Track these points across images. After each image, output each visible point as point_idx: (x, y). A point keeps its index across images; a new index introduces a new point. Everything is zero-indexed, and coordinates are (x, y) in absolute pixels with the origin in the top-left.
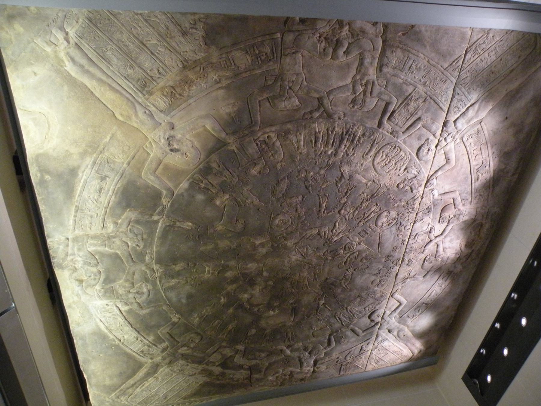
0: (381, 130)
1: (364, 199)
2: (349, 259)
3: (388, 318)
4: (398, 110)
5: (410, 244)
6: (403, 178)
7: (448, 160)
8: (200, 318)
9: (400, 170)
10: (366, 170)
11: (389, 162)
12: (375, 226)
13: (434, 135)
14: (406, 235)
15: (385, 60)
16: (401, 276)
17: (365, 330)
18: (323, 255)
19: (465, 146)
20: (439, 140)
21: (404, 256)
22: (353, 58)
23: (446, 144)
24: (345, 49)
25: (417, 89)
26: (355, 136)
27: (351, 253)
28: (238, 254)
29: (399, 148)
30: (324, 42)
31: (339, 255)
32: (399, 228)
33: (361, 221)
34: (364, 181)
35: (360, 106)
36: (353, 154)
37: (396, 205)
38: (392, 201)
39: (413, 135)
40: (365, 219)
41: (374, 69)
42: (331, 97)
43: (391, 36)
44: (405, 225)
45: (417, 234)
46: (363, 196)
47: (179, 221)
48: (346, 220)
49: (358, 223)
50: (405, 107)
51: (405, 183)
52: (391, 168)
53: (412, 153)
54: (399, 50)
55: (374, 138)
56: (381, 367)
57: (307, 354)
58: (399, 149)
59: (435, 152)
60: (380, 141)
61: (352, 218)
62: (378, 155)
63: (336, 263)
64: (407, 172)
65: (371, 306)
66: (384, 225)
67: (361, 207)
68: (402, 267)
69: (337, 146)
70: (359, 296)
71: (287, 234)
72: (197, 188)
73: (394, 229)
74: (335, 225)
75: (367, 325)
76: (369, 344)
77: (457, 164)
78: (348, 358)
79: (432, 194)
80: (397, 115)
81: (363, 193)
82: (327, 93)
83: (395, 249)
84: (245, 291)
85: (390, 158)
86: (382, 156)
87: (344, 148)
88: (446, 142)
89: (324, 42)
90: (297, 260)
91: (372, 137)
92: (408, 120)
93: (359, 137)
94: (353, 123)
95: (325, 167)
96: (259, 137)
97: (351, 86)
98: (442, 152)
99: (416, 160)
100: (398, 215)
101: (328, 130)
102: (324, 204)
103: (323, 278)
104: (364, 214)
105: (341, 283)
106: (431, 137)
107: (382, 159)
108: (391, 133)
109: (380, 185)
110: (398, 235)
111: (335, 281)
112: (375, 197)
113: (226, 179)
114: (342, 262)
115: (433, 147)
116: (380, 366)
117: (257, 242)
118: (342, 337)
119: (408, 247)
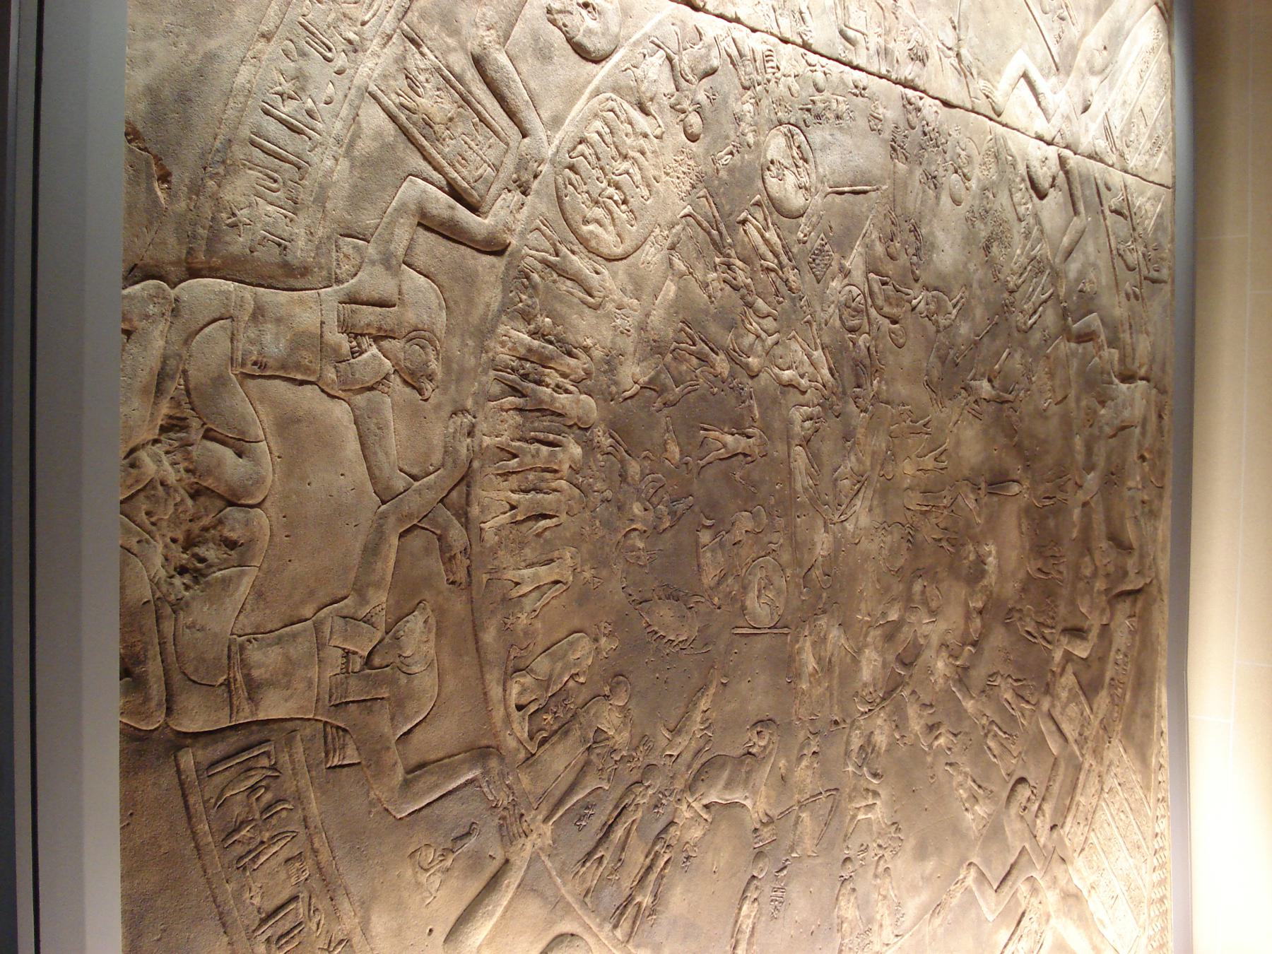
0: (514, 241)
2: (886, 309)
3: (1053, 121)
4: (449, 169)
8: (975, 799)
9: (646, 136)
10: (637, 285)
11: (618, 187)
12: (803, 220)
15: (267, 254)
16: (952, 88)
17: (1074, 204)
18: (865, 411)
22: (259, 407)
24: (229, 454)
25: (373, 88)
27: (869, 300)
28: (836, 723)
30: (201, 551)
31: (873, 350)
32: (818, 117)
33: (786, 282)
34: (670, 289)
35: (430, 349)
36: (586, 349)
37: (750, 138)
38: (737, 156)
40: (780, 263)
41: (302, 302)
42: (400, 482)
43: (172, 241)
44: (812, 90)
46: (716, 284)
49: (790, 289)
50: (437, 139)
51: (686, 104)
52: (638, 178)
53: (591, 87)
54: (228, 195)
56: (1170, 127)
57: (1103, 412)
64: (652, 100)
65: (1018, 196)
66: (805, 180)
67: (747, 286)
68: (927, 87)
70: (987, 248)
74: (790, 385)
75: (1062, 200)
76: (1110, 184)
78: (1132, 258)
80: (465, 172)
82: (384, 503)
84: (930, 671)
85: (605, 183)
87: (567, 391)
89: (201, 551)
91: (535, 276)
92: (482, 120)
93: (532, 334)
94: (485, 372)
97: (360, 400)
101: (506, 475)
107: (607, 221)
109: (685, 216)
111: (938, 349)
112: (720, 234)
116: (1167, 134)
118: (1081, 291)
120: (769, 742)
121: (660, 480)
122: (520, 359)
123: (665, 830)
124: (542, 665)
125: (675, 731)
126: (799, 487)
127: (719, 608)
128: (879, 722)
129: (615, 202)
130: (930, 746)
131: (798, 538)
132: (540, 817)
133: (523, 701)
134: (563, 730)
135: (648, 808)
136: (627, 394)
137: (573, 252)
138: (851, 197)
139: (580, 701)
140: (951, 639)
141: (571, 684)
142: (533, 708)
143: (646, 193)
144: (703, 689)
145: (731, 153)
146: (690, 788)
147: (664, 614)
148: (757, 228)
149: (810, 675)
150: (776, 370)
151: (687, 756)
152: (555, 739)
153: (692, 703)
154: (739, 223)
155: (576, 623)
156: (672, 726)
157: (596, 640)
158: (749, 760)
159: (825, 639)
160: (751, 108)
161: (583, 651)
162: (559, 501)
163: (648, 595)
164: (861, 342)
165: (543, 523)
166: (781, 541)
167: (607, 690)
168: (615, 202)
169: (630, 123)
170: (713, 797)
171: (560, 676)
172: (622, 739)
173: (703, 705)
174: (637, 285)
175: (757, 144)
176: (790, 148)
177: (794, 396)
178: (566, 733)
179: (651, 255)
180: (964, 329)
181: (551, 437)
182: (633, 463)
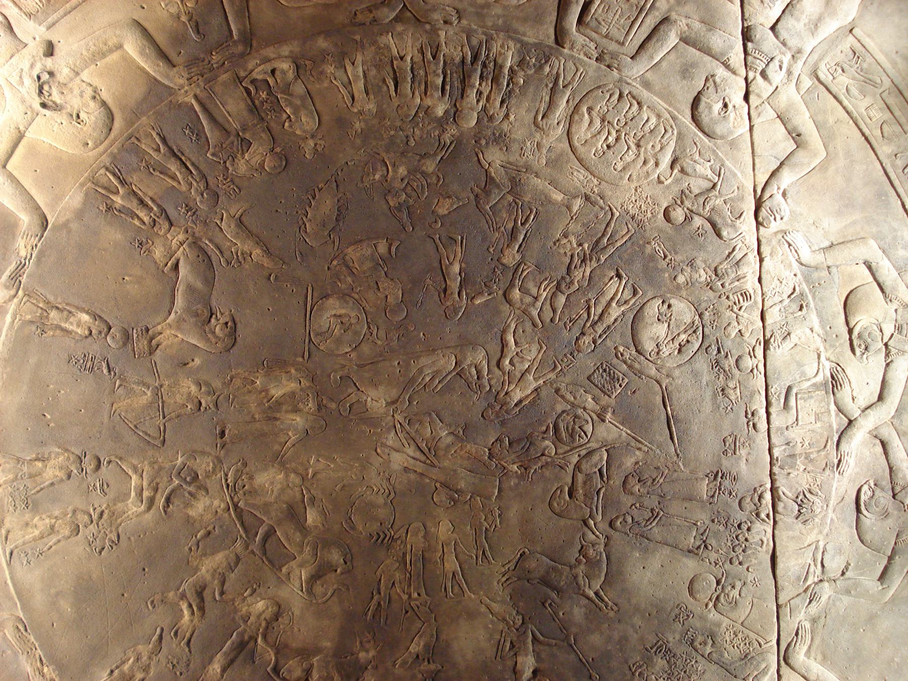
1: (572, 256)
2: (580, 478)
5: (779, 429)
6: (676, 189)
7: (797, 137)
10: (555, 162)
13: (727, 66)
14: (752, 395)
16: (789, 565)
18: (491, 456)
19: (835, 97)
20: (746, 79)
21: (771, 474)
23: (772, 89)
26: (498, 67)
27: (583, 453)
28: (223, 434)
29: (634, 98)
33: (583, 334)
34: (558, 197)
36: (507, 116)
37: (681, 279)
39: (664, 64)
45: (789, 389)
47: (57, 308)
48: (534, 325)
49: (577, 339)
51: (688, 204)
55: (555, 72)
58: (635, 103)
59: (749, 114)
60: (573, 79)
61: (552, 320)
62: (576, 117)
63: (538, 490)
64: (682, 171)
66: (665, 351)
67: (572, 282)
68: (780, 525)
69: (457, 93)
71: (360, 366)
72: (103, 208)
73: (702, 365)
74: (504, 345)
77: (831, 148)
79: (790, 245)
81: (566, 236)
83: (730, 446)
84: (254, 585)
85: (617, 128)
86: (591, 122)
87: (478, 101)
88: (771, 84)
90: (406, 469)
91: (547, 69)
93: (511, 68)
95: (435, 154)
96: (252, 71)
98: (769, 113)
99: (695, 134)
100: (700, 316)
102: (456, 268)
103: (510, 554)
104: (589, 308)
105: (575, 577)
106: (721, 72)
108: (597, 59)
110: (723, 390)
113: (175, 184)
114: (561, 489)
115: (737, 98)
117: (277, 392)
119: (774, 440)
120: (217, 337)
121: (423, 193)
122: (495, 60)
123: (168, 218)
124: (299, 89)
125: (240, 222)
126: (424, 361)
127: (329, 268)
128: (216, 503)
129: (607, 138)
130: (183, 596)
131: (381, 364)
132: (198, 92)
133: (277, 73)
134: (254, 109)
135: (187, 198)
136: (481, 156)
137: (568, 102)
138: (663, 417)
139: (273, 124)
140: (283, 620)
141: (285, 116)
142: (271, 81)
143: (619, 166)
144: (268, 252)
145: (665, 257)
146: (195, 243)
147: (327, 205)
148: (617, 291)
149: (267, 391)
150: (513, 326)
151: (219, 239)
152: (249, 102)
153: (260, 241)
154: (617, 270)
155: (325, 118)
156: (244, 219)
157: (313, 137)
158: (207, 314)
159: (296, 410)
160: (703, 279)
161: (307, 122)
162: (406, 96)
163: (341, 189)
164: (547, 442)
165: (392, 88)
166: (379, 342)
167: (278, 150)
168: (607, 138)
169: (661, 149)
170: (183, 270)
171: (290, 104)
172: (242, 167)
173: (257, 252)
174: (555, 162)
175: (678, 288)
177: (495, 348)
178: (251, 111)
179: (579, 177)
180: (578, 613)
181: (448, 88)
182: (434, 166)
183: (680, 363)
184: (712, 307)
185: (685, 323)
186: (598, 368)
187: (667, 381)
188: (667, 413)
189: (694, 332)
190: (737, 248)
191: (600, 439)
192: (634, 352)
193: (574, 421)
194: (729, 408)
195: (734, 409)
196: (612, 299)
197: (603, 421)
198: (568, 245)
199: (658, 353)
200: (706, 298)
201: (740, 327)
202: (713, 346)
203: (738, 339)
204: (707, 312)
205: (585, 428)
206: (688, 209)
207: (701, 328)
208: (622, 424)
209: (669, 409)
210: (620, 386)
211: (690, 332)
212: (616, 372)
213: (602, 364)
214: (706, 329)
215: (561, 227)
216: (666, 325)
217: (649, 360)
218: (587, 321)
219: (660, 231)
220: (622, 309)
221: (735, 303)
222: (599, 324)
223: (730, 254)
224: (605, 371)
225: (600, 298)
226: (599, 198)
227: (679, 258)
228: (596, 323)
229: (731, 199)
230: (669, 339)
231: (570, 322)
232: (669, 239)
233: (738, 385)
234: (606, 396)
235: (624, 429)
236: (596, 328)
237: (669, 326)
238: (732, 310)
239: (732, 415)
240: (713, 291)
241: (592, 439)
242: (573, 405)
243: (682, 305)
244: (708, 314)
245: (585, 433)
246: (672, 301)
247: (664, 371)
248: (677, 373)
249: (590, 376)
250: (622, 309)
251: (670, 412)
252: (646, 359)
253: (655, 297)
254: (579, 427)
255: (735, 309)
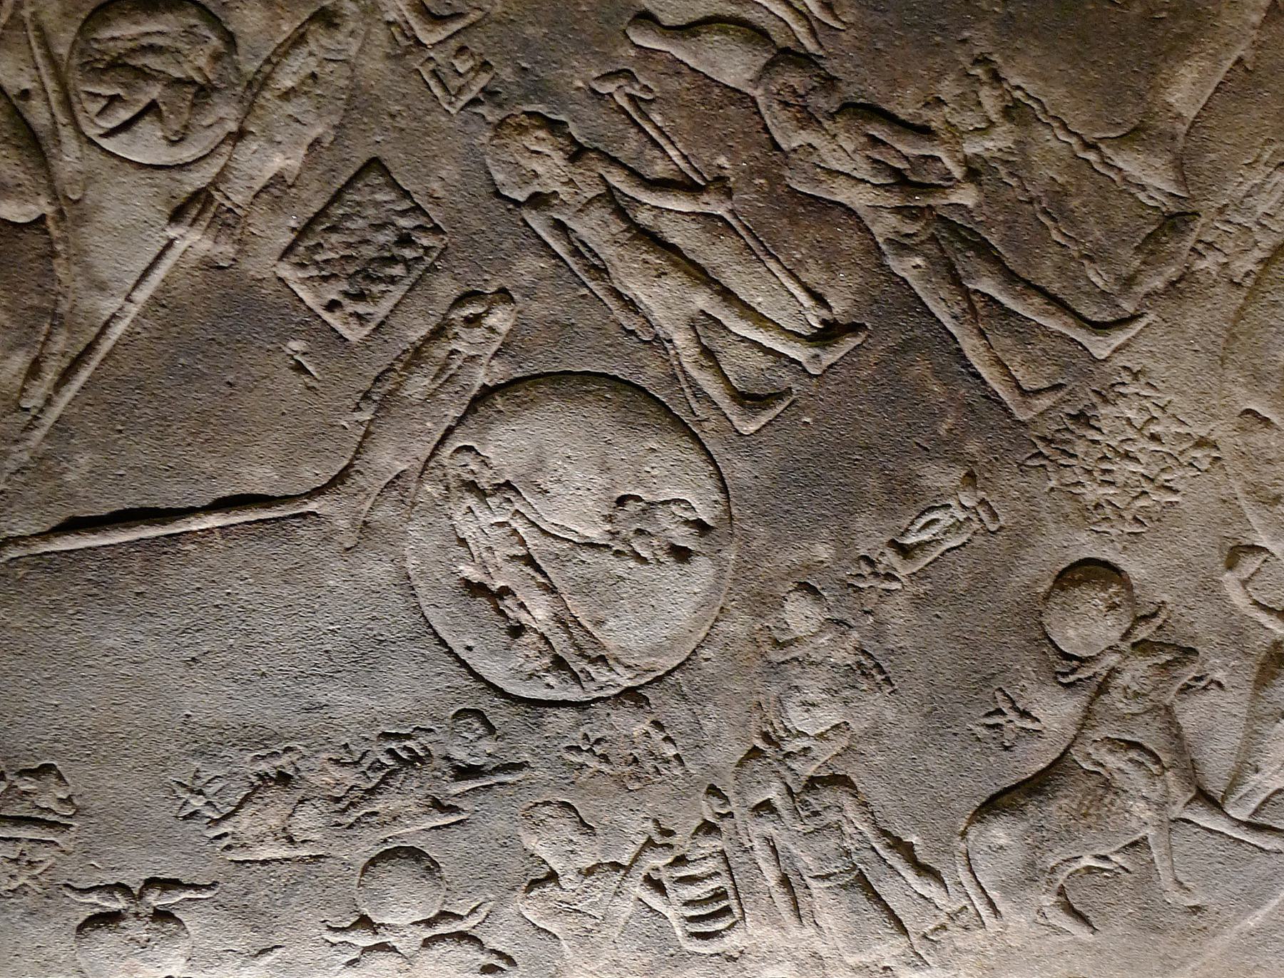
1: (924, 132)
33: (577, 154)
49: (554, 127)
51: (1136, 671)
67: (808, 119)
81: (1013, 111)
100: (632, 695)
104: (689, 188)
110: (283, 779)
145: (905, 552)
148: (761, 320)
154: (854, 328)
160: (797, 718)
176: (562, 622)
183: (422, 588)
184: (670, 751)
185: (599, 623)
186: (417, 209)
187: (343, 523)
188: (192, 511)
189: (559, 663)
190: (931, 890)
191: (92, 194)
192: (481, 377)
193: (192, 82)
194: (197, 803)
195: (192, 825)
196: (727, 295)
197: (176, 216)
198: (969, 120)
199: (472, 487)
200: (709, 726)
201: (569, 881)
202: (488, 745)
203: (515, 867)
204: (646, 726)
205: (149, 129)
206: (1113, 672)
207: (574, 694)
208: (154, 300)
209: (214, 521)
210: (332, 306)
211: (560, 643)
212: (397, 292)
213: (437, 230)
214: (566, 717)
215: (1055, 96)
216: (595, 533)
217: (442, 442)
218: (634, 174)
219: (1020, 538)
220: (681, 339)
221: (681, 861)
222: (617, 226)
223: (907, 851)
224: (405, 240)
225: (730, 241)
226: (1172, 272)
227: (897, 614)
228: (621, 213)
229: (1148, 875)
230: (534, 542)
231: (631, 98)
232: (984, 581)
233: (304, 852)
234: (286, 239)
235: (133, 310)
236: (599, 213)
237: (592, 545)
238: (650, 843)
239: (163, 812)
240: (741, 764)
241: (95, 156)
242: (260, 83)
243: (685, 613)
244: (637, 730)
245: (126, 126)
246: (702, 568)
247: (385, 513)
248: (377, 570)
249: (386, 172)
250: (681, 339)
251: (196, 524)
252: (449, 431)
253: (724, 489)
254: (152, 108)
255: (657, 861)
